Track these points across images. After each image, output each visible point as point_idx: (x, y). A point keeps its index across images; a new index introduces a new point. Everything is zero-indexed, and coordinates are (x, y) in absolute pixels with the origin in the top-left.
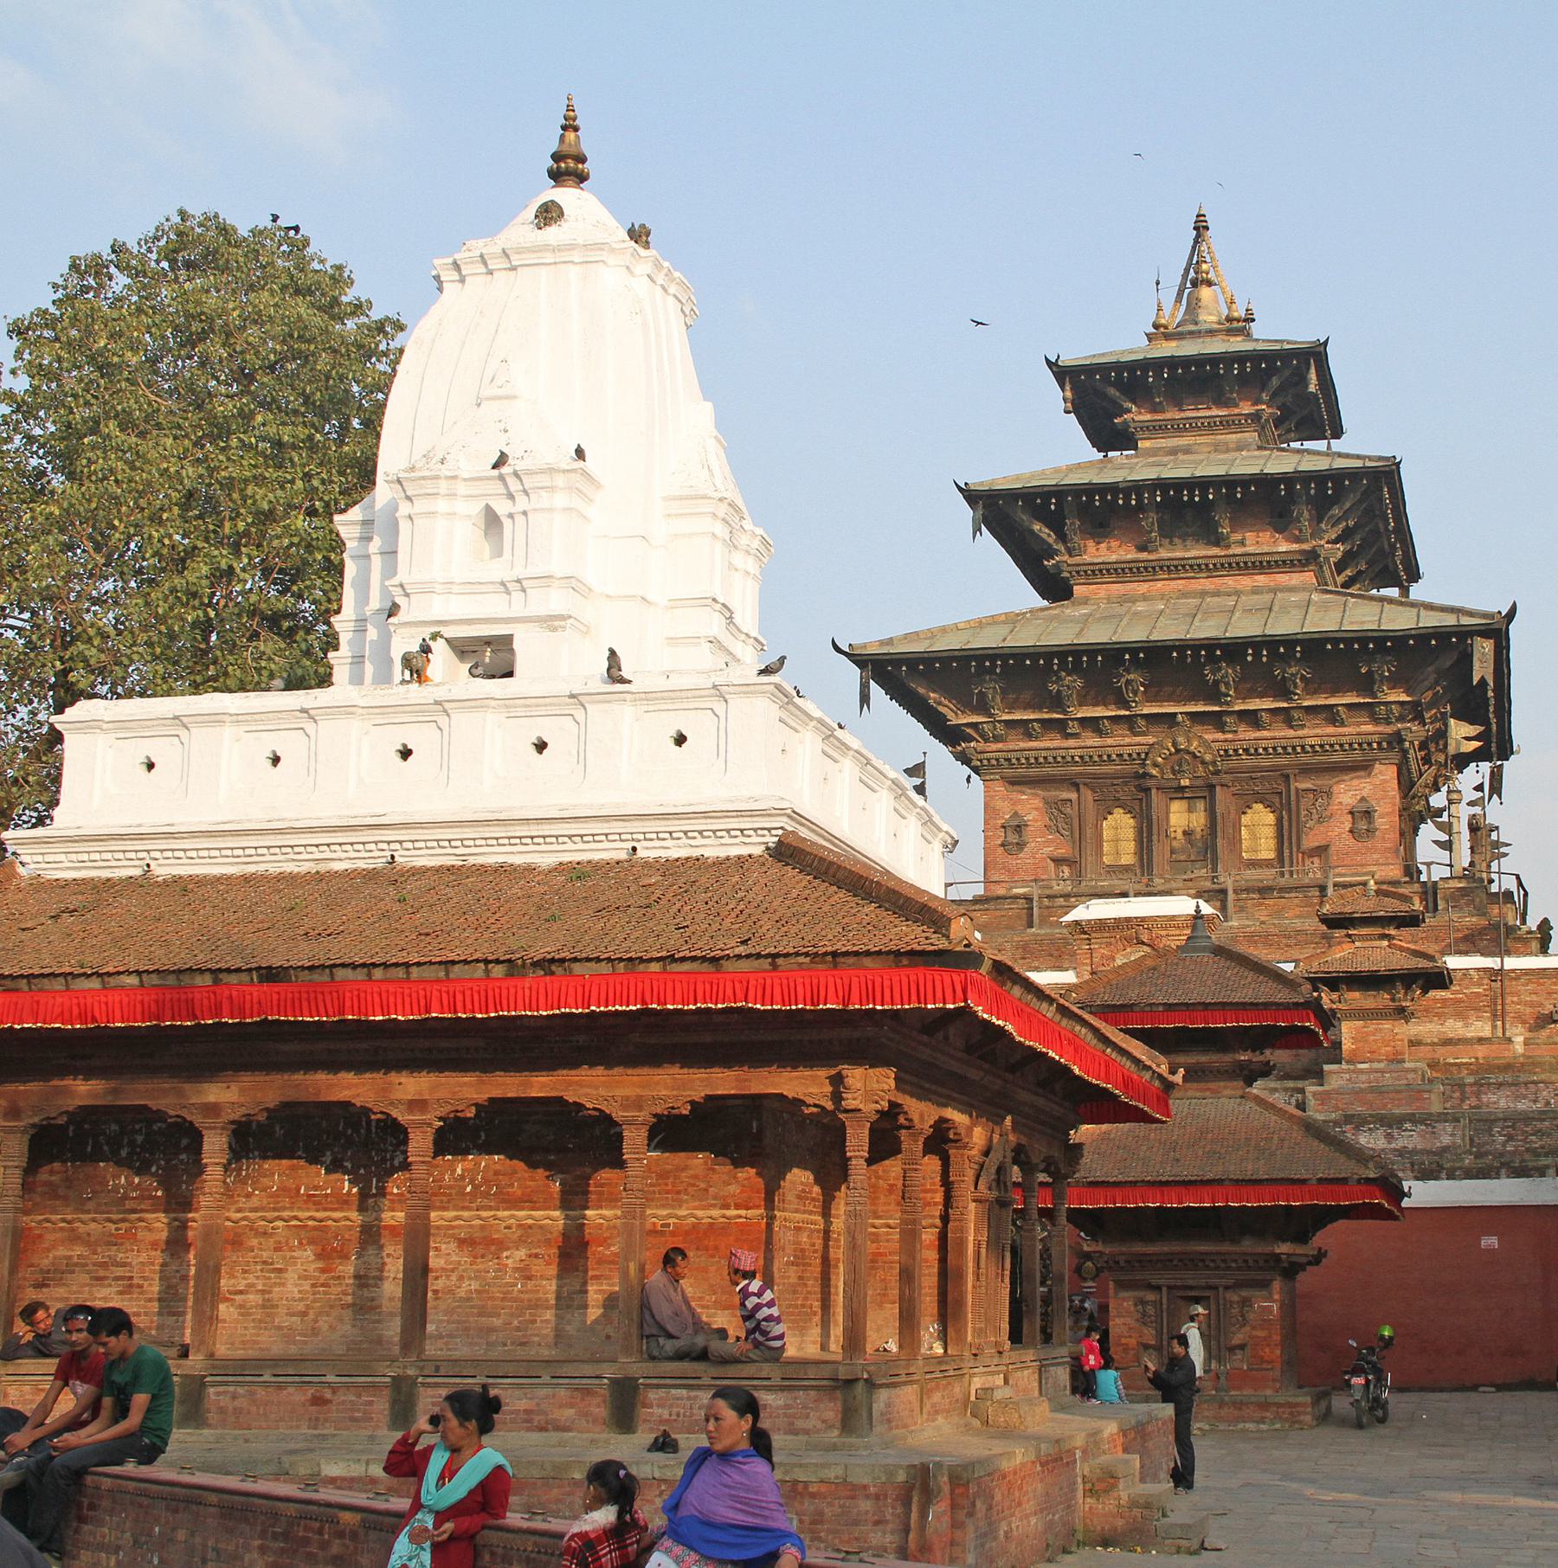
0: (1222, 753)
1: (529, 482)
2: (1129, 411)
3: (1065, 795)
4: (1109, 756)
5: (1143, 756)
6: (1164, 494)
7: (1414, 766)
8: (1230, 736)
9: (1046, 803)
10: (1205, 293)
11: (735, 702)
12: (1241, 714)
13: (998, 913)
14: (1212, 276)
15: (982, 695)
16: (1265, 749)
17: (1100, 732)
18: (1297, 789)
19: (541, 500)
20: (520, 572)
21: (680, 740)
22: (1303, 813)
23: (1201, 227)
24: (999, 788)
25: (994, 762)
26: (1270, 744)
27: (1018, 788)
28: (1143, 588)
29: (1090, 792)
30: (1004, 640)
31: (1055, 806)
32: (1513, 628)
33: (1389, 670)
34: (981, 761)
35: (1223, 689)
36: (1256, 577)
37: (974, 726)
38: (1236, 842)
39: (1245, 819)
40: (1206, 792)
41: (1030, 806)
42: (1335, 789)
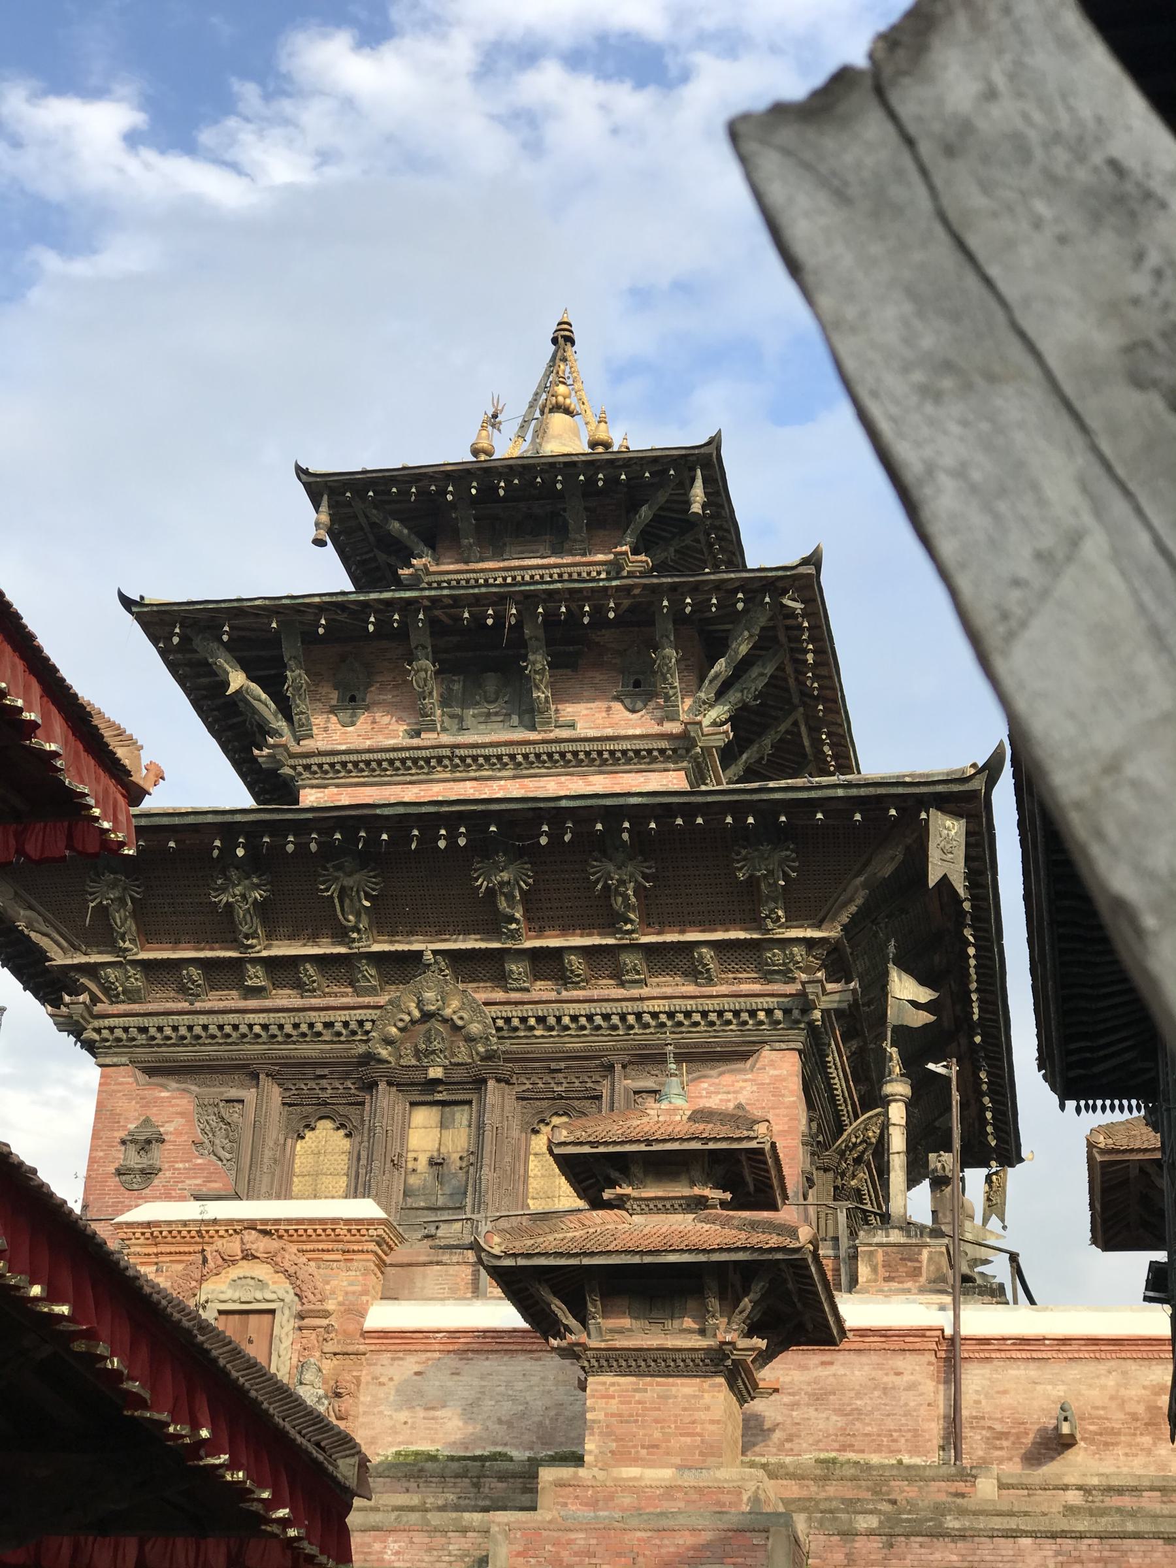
0: (500, 1023)
3: (233, 1093)
4: (311, 1026)
12: (536, 955)
14: (572, 403)
15: (102, 912)
16: (574, 1018)
17: (300, 986)
24: (127, 1078)
25: (119, 1033)
26: (584, 1009)
27: (155, 1080)
33: (786, 877)
34: (98, 1031)
35: (503, 904)
36: (592, 779)
37: (91, 970)
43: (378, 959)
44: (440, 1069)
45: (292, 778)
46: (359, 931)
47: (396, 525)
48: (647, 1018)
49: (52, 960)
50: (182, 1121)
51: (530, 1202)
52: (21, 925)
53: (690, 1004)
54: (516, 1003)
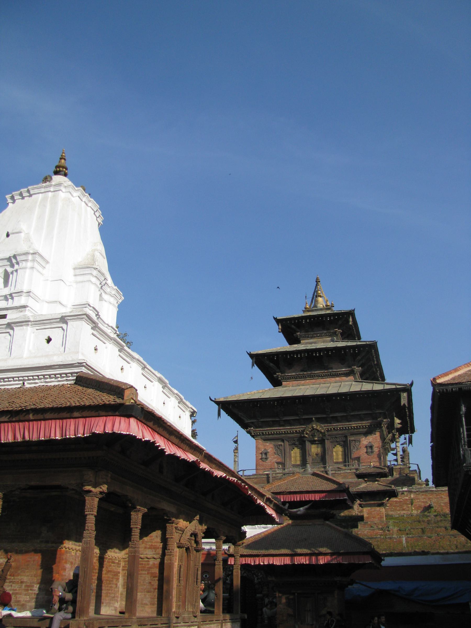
0: (327, 429)
1: (19, 258)
2: (298, 332)
3: (280, 443)
4: (293, 431)
5: (303, 431)
6: (308, 354)
7: (385, 433)
8: (329, 425)
9: (274, 446)
10: (320, 299)
11: (70, 323)
13: (260, 479)
16: (340, 428)
18: (350, 440)
19: (22, 265)
20: (13, 291)
21: (49, 340)
22: (352, 447)
23: (317, 281)
24: (260, 441)
25: (258, 434)
26: (341, 426)
27: (266, 441)
28: (303, 382)
29: (287, 442)
30: (261, 396)
31: (277, 447)
32: (413, 389)
34: (254, 433)
37: (252, 423)
38: (332, 456)
39: (334, 450)
40: (322, 442)
41: (269, 447)
42: (361, 440)
43: (304, 419)
44: (316, 438)
45: (281, 380)
47: (293, 326)
48: (353, 427)
49: (245, 421)
50: (271, 449)
51: (334, 460)
52: (239, 416)
53: (360, 425)
54: (329, 426)
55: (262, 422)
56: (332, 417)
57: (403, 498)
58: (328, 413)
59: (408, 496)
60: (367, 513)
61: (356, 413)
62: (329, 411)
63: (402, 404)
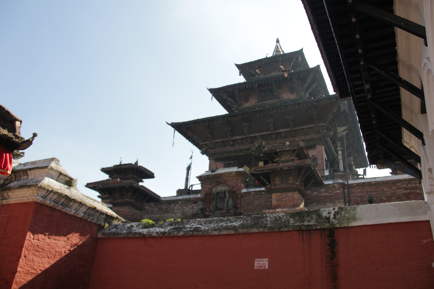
2: (256, 76)
3: (230, 162)
4: (241, 150)
8: (274, 141)
24: (213, 161)
37: (206, 144)
43: (251, 137)
46: (247, 133)
55: (214, 143)
56: (276, 133)
57: (333, 192)
58: (272, 129)
59: (340, 189)
60: (276, 200)
61: (299, 128)
62: (273, 127)
63: (342, 110)
